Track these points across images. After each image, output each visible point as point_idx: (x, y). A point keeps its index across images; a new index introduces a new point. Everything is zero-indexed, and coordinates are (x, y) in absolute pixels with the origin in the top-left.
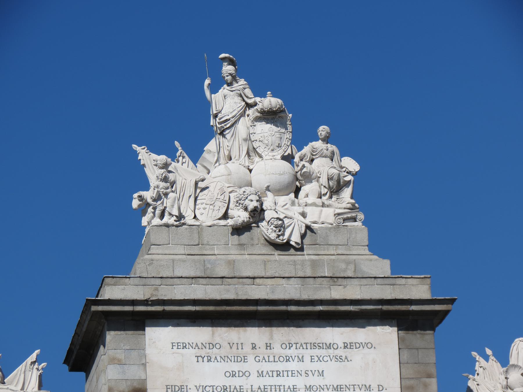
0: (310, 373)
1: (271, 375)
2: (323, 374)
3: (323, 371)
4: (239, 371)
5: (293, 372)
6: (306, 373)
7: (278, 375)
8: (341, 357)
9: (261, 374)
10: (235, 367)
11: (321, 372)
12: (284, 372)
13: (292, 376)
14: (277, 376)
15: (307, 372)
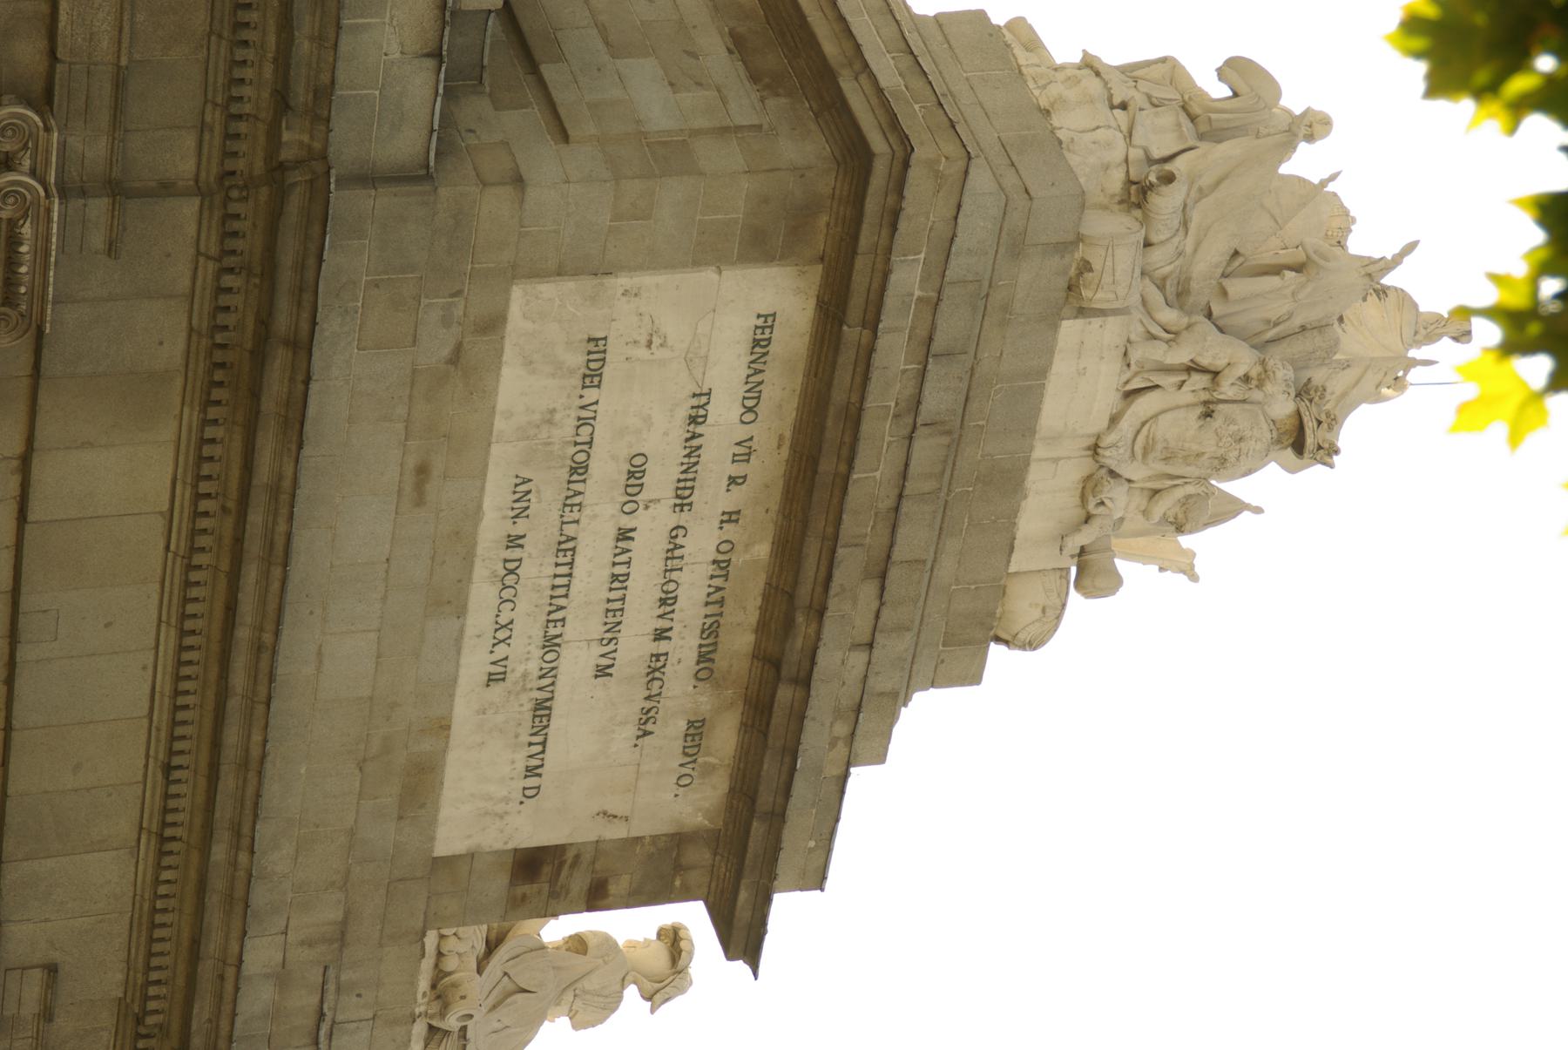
0: (611, 647)
1: (618, 559)
2: (600, 676)
3: (611, 675)
4: (642, 485)
5: (620, 613)
6: (611, 640)
7: (615, 578)
8: (644, 711)
9: (624, 535)
10: (661, 480)
11: (608, 671)
12: (624, 591)
13: (608, 610)
14: (613, 575)
15: (614, 641)
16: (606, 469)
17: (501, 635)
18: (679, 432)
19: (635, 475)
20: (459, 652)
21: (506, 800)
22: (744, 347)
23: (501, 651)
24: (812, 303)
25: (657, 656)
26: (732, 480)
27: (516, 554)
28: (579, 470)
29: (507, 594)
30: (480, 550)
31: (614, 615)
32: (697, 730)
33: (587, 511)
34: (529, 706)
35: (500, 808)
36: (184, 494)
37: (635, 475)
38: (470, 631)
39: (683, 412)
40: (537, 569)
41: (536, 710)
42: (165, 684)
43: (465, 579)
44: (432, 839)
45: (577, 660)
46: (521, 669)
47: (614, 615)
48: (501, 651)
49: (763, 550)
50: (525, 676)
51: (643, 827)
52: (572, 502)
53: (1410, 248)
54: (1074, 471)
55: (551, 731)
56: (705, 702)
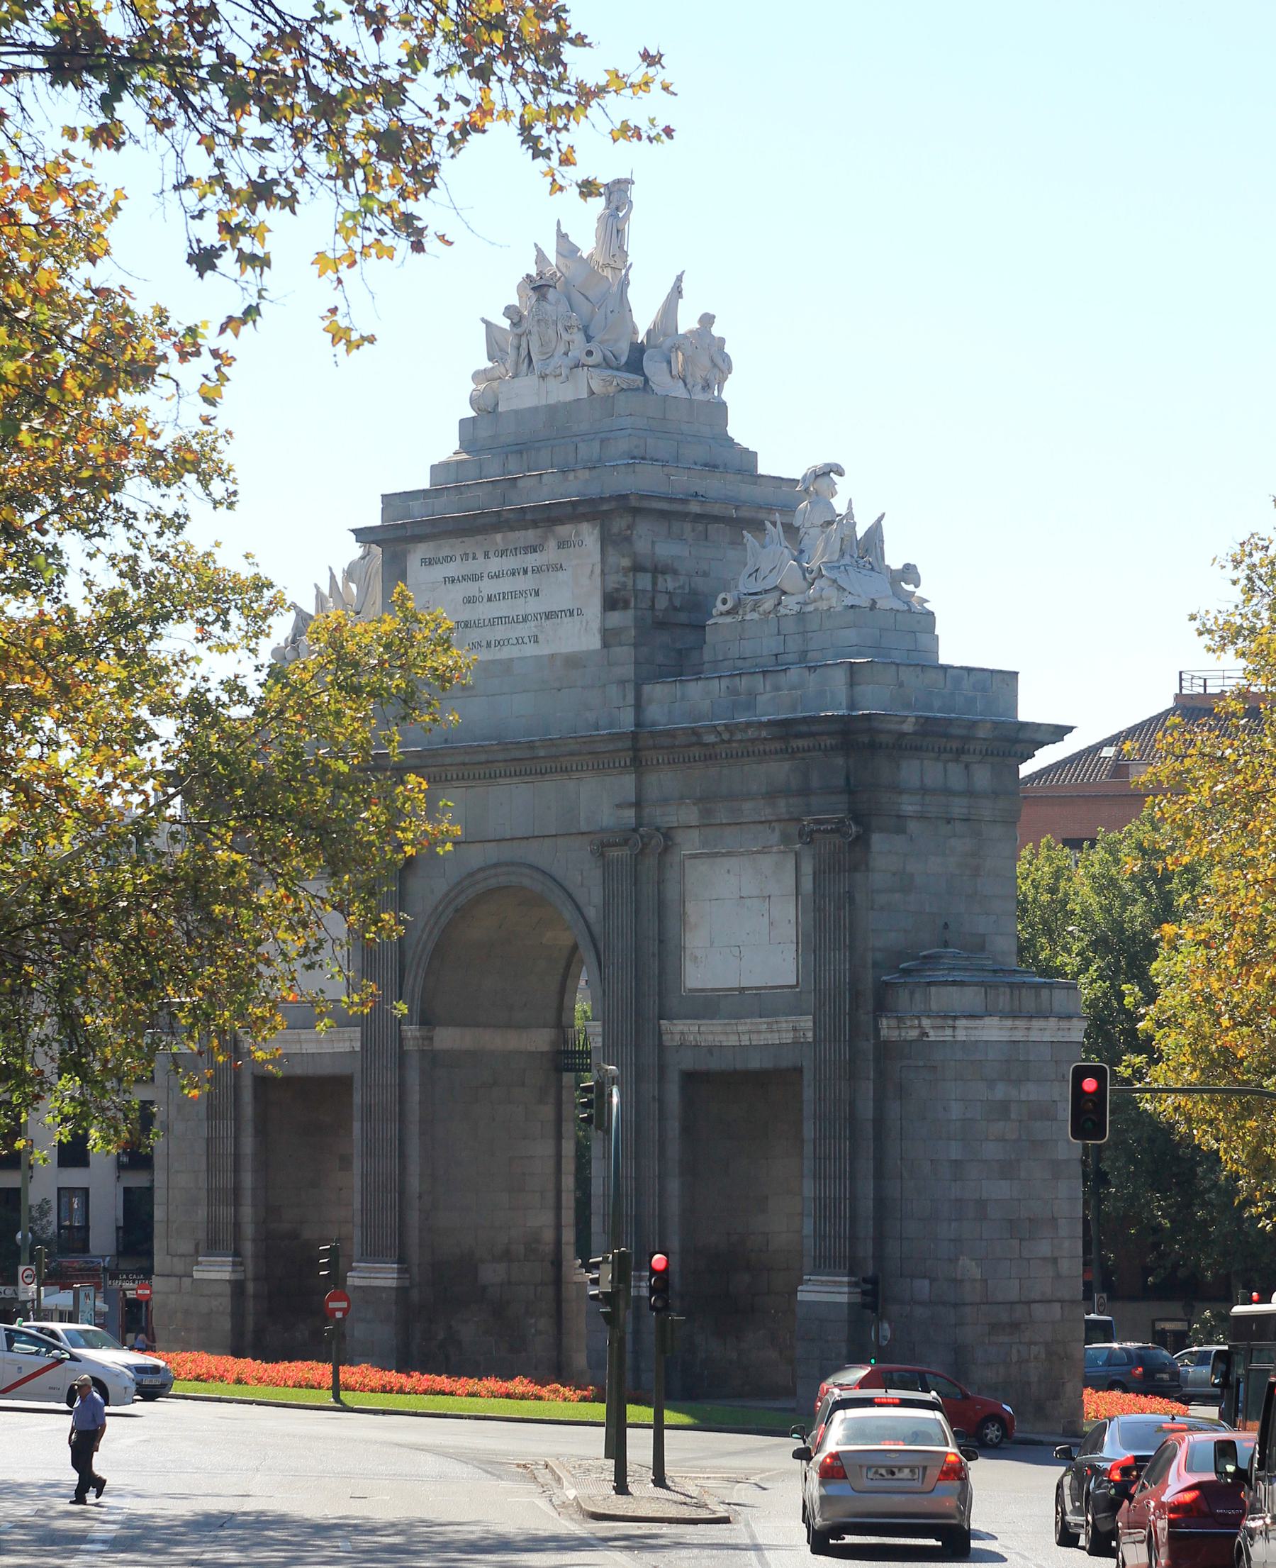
10: (471, 588)
16: (467, 614)
17: (520, 641)
18: (457, 586)
19: (470, 600)
20: (526, 657)
21: (581, 622)
22: (431, 568)
23: (526, 640)
24: (419, 545)
25: (533, 570)
26: (474, 558)
27: (493, 643)
28: (467, 625)
29: (506, 643)
30: (490, 658)
31: (515, 595)
32: (562, 545)
33: (482, 617)
34: (548, 622)
35: (584, 624)
36: (455, 784)
37: (470, 600)
38: (519, 655)
39: (450, 586)
40: (500, 632)
41: (547, 618)
42: (515, 780)
43: (500, 662)
44: (594, 651)
45: (532, 606)
46: (534, 629)
47: (515, 595)
48: (526, 640)
49: (499, 537)
50: (536, 627)
51: (597, 557)
52: (477, 624)
53: (536, 245)
54: (552, 383)
55: (556, 610)
56: (552, 544)
